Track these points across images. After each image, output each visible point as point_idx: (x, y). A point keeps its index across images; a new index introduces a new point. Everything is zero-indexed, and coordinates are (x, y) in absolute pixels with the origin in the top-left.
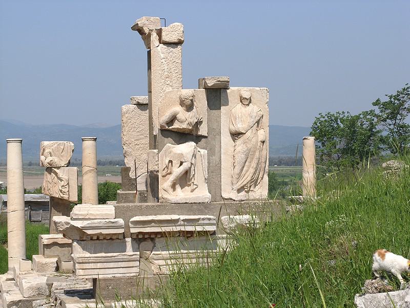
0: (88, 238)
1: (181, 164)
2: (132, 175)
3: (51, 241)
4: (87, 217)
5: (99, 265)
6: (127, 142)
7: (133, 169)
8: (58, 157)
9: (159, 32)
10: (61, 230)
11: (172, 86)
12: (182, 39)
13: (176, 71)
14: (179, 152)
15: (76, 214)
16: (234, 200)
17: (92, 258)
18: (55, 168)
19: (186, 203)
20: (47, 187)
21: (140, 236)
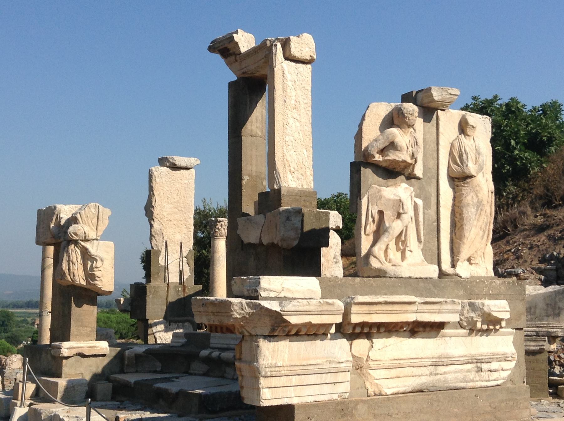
0: (284, 331)
1: (399, 215)
3: (74, 351)
4: (282, 295)
5: (295, 380)
6: (158, 217)
7: (163, 253)
8: (89, 226)
9: (286, 44)
10: (238, 316)
11: (299, 121)
12: (315, 57)
13: (305, 101)
14: (392, 197)
15: (265, 290)
16: (461, 277)
17: (286, 369)
18: (82, 240)
19: (410, 278)
20: (69, 269)
21: (358, 330)
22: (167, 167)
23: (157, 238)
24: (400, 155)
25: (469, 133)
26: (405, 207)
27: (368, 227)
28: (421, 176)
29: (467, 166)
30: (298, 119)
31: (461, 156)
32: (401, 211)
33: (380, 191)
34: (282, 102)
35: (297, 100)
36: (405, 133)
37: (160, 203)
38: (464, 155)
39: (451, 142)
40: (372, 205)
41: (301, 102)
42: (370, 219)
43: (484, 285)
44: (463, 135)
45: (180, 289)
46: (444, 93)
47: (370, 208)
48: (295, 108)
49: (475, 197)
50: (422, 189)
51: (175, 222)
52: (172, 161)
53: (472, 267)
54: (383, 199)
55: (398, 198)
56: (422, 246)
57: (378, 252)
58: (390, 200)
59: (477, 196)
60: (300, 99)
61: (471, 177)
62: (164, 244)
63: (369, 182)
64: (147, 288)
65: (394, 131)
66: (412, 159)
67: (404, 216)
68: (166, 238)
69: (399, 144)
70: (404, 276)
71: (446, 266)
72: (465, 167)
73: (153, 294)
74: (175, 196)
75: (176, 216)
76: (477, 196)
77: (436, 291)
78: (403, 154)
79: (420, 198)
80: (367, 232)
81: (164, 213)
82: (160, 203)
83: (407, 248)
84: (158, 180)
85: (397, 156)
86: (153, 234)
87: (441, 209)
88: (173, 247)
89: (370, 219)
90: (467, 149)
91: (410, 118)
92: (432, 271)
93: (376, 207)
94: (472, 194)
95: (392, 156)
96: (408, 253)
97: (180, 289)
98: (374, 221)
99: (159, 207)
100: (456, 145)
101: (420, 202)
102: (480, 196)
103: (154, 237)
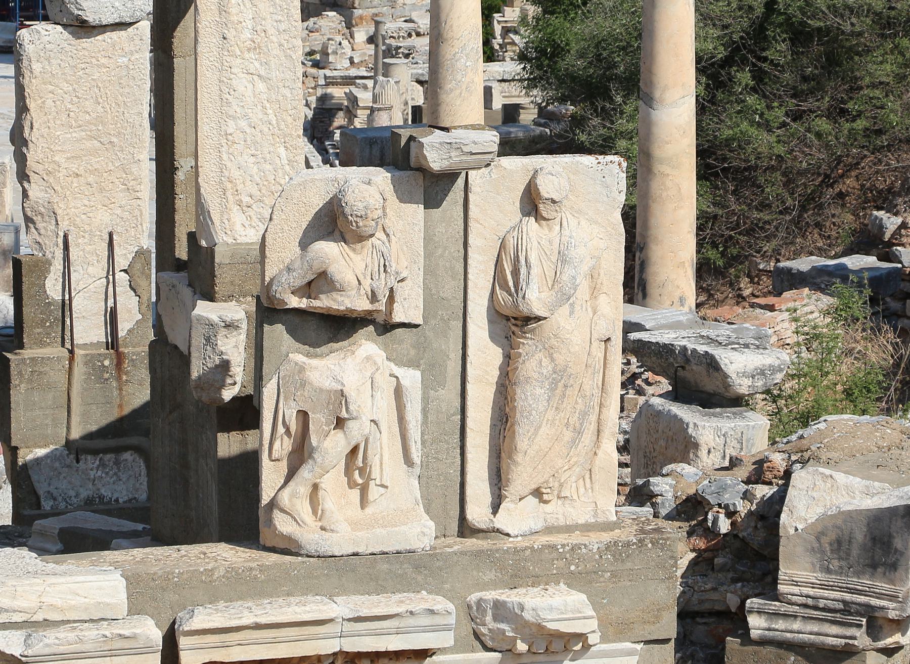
1: (340, 423)
2: (53, 288)
6: (39, 168)
7: (57, 266)
13: (283, 27)
14: (328, 384)
16: (508, 535)
22: (65, 26)
23: (40, 225)
24: (340, 299)
25: (544, 214)
26: (351, 407)
27: (277, 445)
28: (419, 321)
29: (524, 298)
30: (262, 73)
31: (516, 273)
32: (344, 414)
33: (302, 369)
34: (216, 40)
35: (259, 28)
36: (354, 250)
37: (45, 131)
38: (523, 270)
39: (502, 235)
40: (286, 399)
41: (271, 31)
42: (281, 430)
43: (555, 555)
44: (533, 219)
45: (107, 363)
46: (453, 154)
47: (281, 405)
48: (255, 48)
49: (546, 362)
50: (422, 346)
51: (91, 179)
52: (76, 12)
53: (548, 508)
54: (307, 387)
55: (340, 388)
56: (417, 470)
57: (290, 500)
58: (321, 390)
59: (552, 360)
60: (269, 25)
61: (538, 319)
62: (60, 241)
63: (284, 349)
64: (12, 365)
65: (328, 251)
66: (372, 303)
67: (350, 424)
68: (64, 225)
69: (337, 277)
70: (337, 554)
71: (478, 511)
72: (520, 299)
73: (30, 381)
74: (89, 104)
75: (94, 160)
76: (552, 360)
77: (419, 578)
78: (349, 297)
79: (418, 367)
80: (275, 455)
81: (56, 158)
82: (45, 131)
83: (372, 483)
84: (36, 67)
85: (334, 300)
86: (29, 214)
87: (469, 387)
88: (88, 248)
89: (281, 430)
90: (533, 259)
91: (361, 224)
92: (420, 532)
93: (293, 404)
94: (537, 356)
95: (324, 302)
96: (374, 492)
97: (107, 363)
98: (288, 432)
99: (41, 143)
100: (511, 243)
101: (411, 378)
102: (560, 358)
103: (34, 223)
